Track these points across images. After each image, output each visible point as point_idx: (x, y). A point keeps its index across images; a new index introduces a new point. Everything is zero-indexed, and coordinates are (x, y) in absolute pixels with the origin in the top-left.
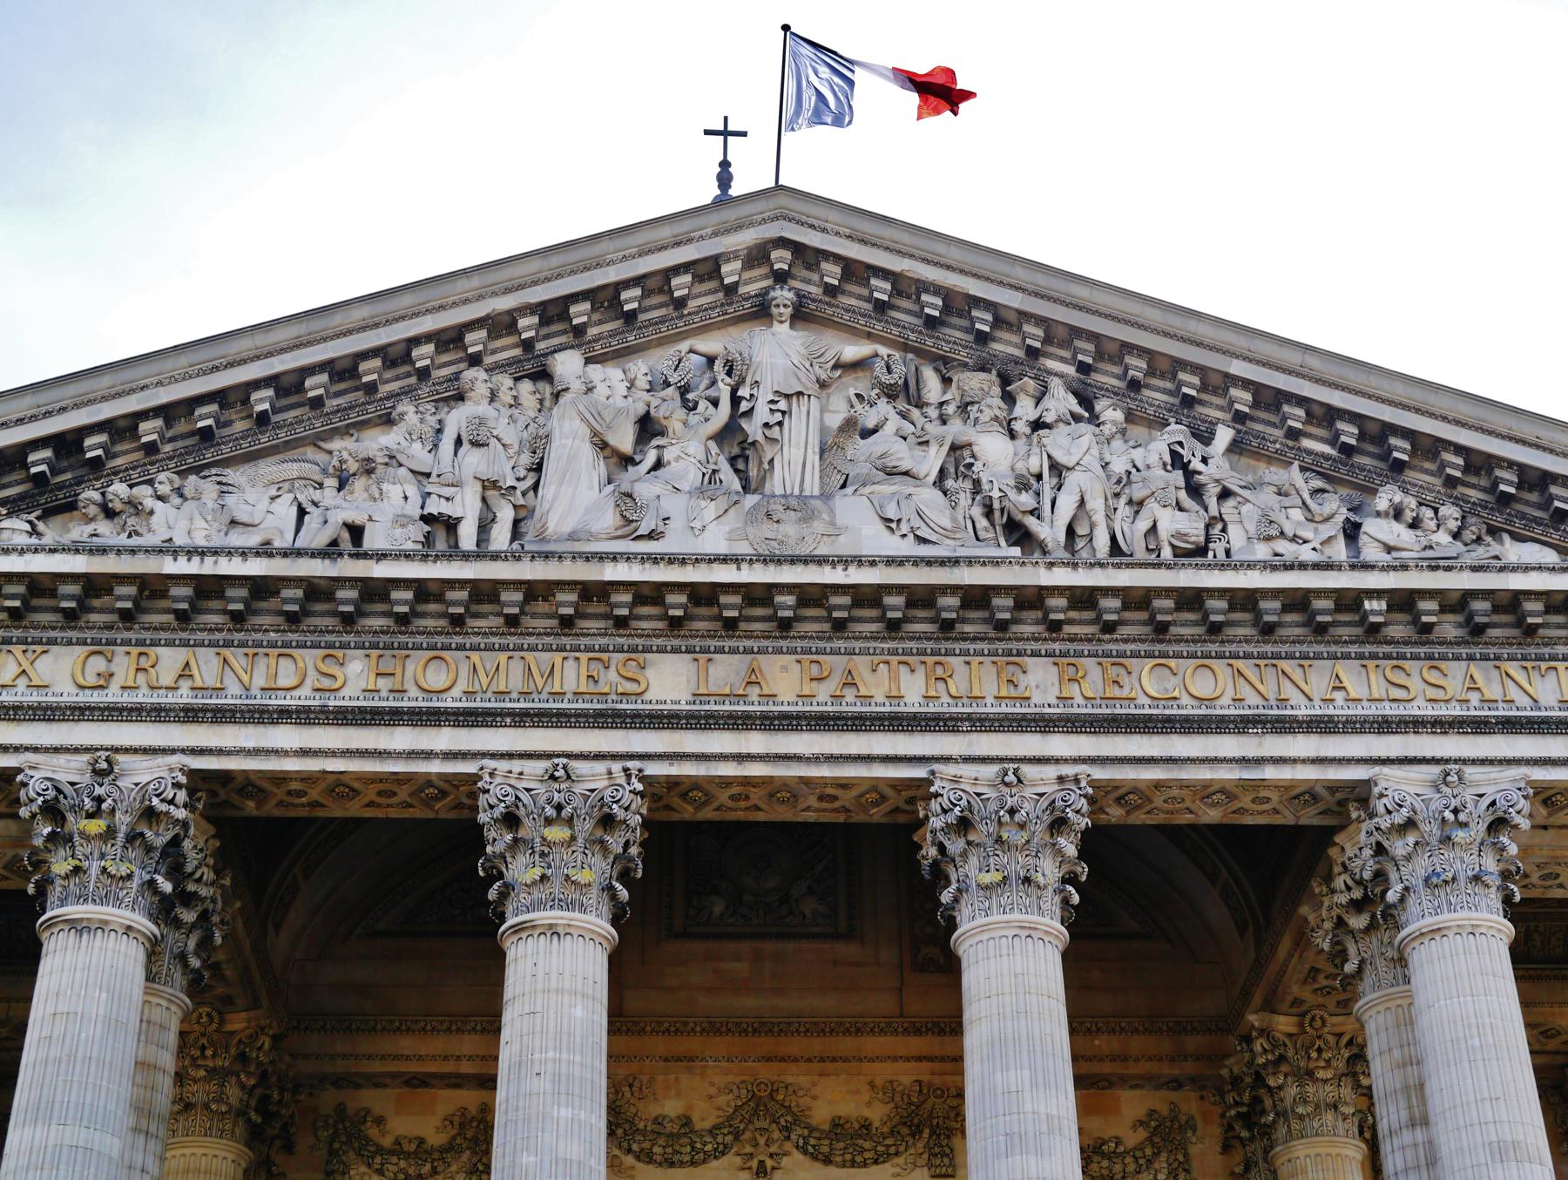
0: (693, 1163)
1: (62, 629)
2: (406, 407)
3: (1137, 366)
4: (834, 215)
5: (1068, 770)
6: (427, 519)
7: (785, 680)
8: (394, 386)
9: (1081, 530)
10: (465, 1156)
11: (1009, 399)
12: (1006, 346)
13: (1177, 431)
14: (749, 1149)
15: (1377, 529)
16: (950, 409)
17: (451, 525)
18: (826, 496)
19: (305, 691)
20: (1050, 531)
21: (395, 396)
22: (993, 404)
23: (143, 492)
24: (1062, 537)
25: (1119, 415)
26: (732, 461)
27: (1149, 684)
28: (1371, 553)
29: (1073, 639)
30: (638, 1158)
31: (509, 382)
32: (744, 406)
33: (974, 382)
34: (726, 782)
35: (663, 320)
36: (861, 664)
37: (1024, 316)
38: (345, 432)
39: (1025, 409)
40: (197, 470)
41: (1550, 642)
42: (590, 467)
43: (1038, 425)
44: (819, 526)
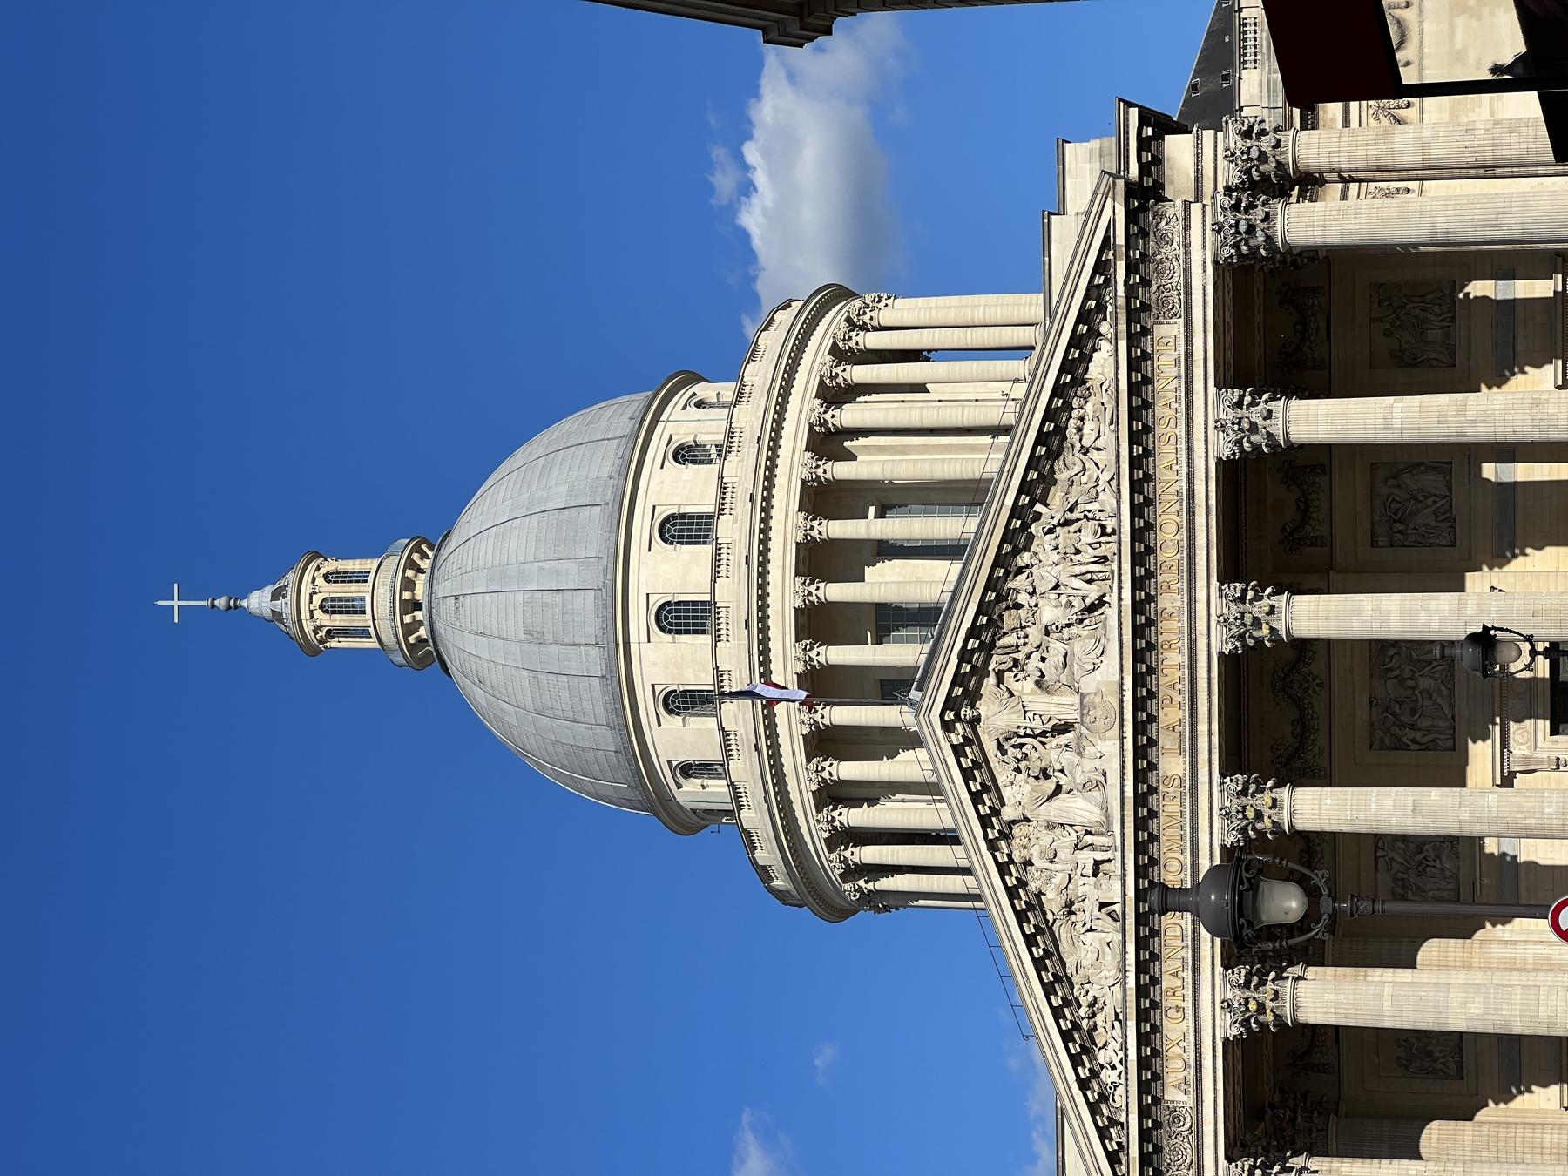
2: (1033, 887)
6: (1095, 875)
7: (1171, 714)
9: (1088, 576)
11: (1018, 606)
15: (1087, 442)
16: (1021, 634)
17: (1097, 864)
18: (1082, 696)
19: (1183, 922)
20: (1093, 593)
23: (1084, 1001)
24: (1092, 587)
25: (1026, 555)
27: (1169, 554)
28: (1099, 444)
31: (1016, 842)
33: (1010, 620)
38: (1044, 913)
39: (1023, 598)
40: (1069, 980)
44: (1097, 700)
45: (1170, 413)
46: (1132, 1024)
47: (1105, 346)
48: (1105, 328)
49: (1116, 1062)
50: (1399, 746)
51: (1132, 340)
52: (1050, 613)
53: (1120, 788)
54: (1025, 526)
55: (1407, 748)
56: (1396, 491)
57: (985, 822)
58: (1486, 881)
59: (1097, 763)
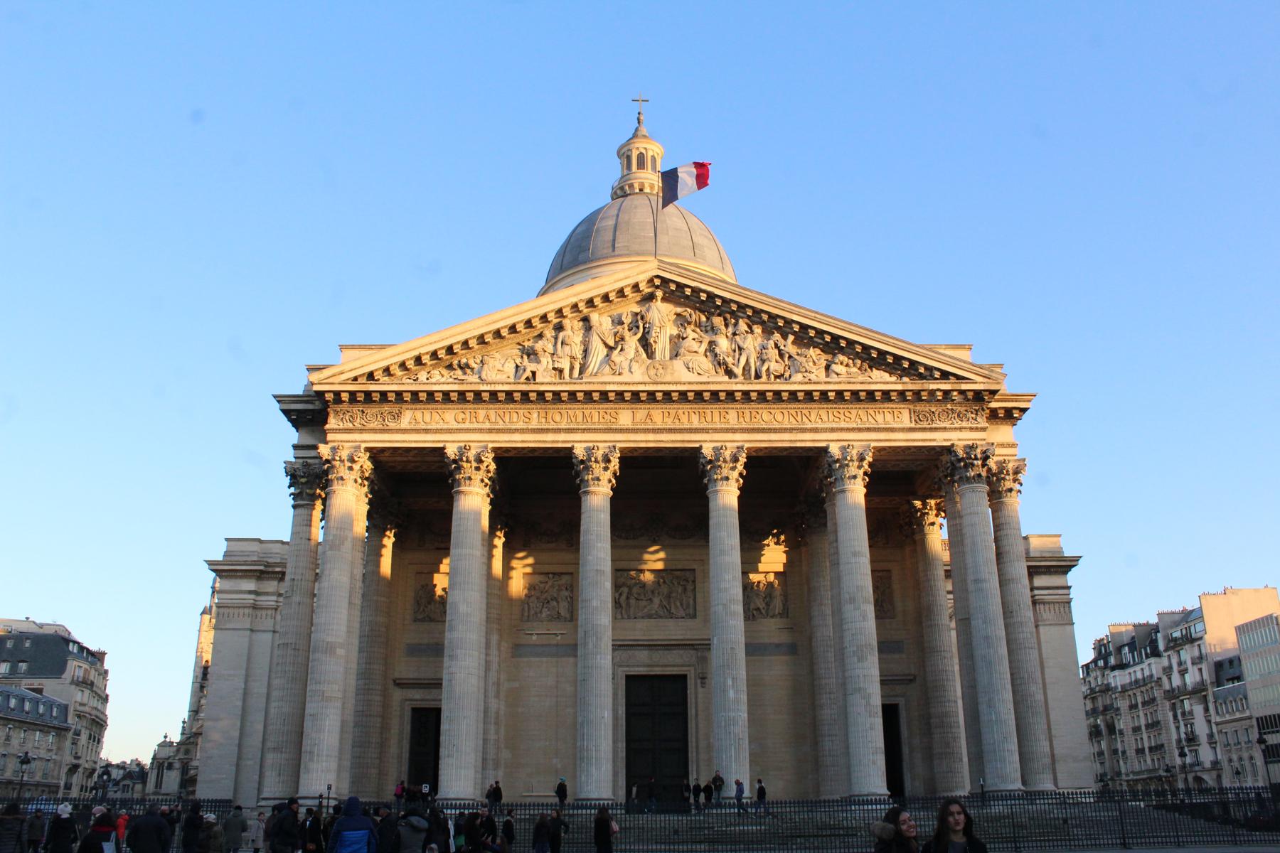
3: (765, 317)
5: (739, 444)
7: (658, 415)
11: (726, 326)
13: (777, 336)
15: (834, 367)
22: (723, 328)
26: (643, 347)
31: (576, 322)
36: (680, 412)
39: (731, 329)
42: (603, 351)
43: (734, 334)
45: (853, 416)
46: (456, 387)
47: (894, 379)
48: (905, 379)
49: (433, 380)
51: (902, 393)
52: (723, 344)
53: (612, 383)
54: (779, 329)
57: (590, 303)
58: (534, 638)
59: (627, 368)
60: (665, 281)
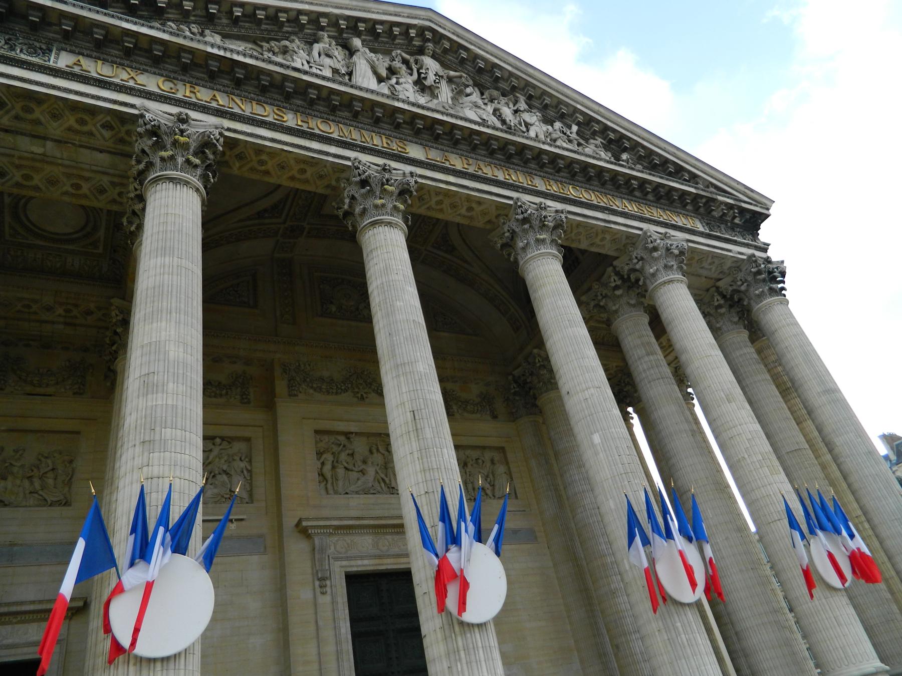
0: (337, 393)
1: (151, 66)
4: (448, 24)
8: (289, 29)
10: (239, 390)
12: (503, 85)
14: (356, 390)
21: (290, 33)
29: (546, 172)
30: (315, 390)
32: (423, 75)
33: (495, 93)
34: (439, 192)
35: (387, 43)
37: (511, 74)
41: (676, 208)
50: (319, 454)
55: (318, 459)
56: (488, 464)
60: (438, 38)
